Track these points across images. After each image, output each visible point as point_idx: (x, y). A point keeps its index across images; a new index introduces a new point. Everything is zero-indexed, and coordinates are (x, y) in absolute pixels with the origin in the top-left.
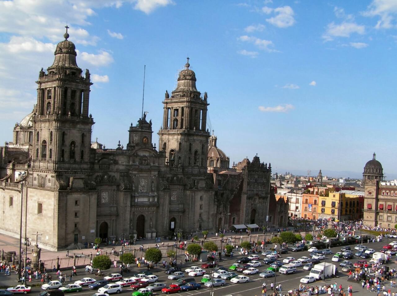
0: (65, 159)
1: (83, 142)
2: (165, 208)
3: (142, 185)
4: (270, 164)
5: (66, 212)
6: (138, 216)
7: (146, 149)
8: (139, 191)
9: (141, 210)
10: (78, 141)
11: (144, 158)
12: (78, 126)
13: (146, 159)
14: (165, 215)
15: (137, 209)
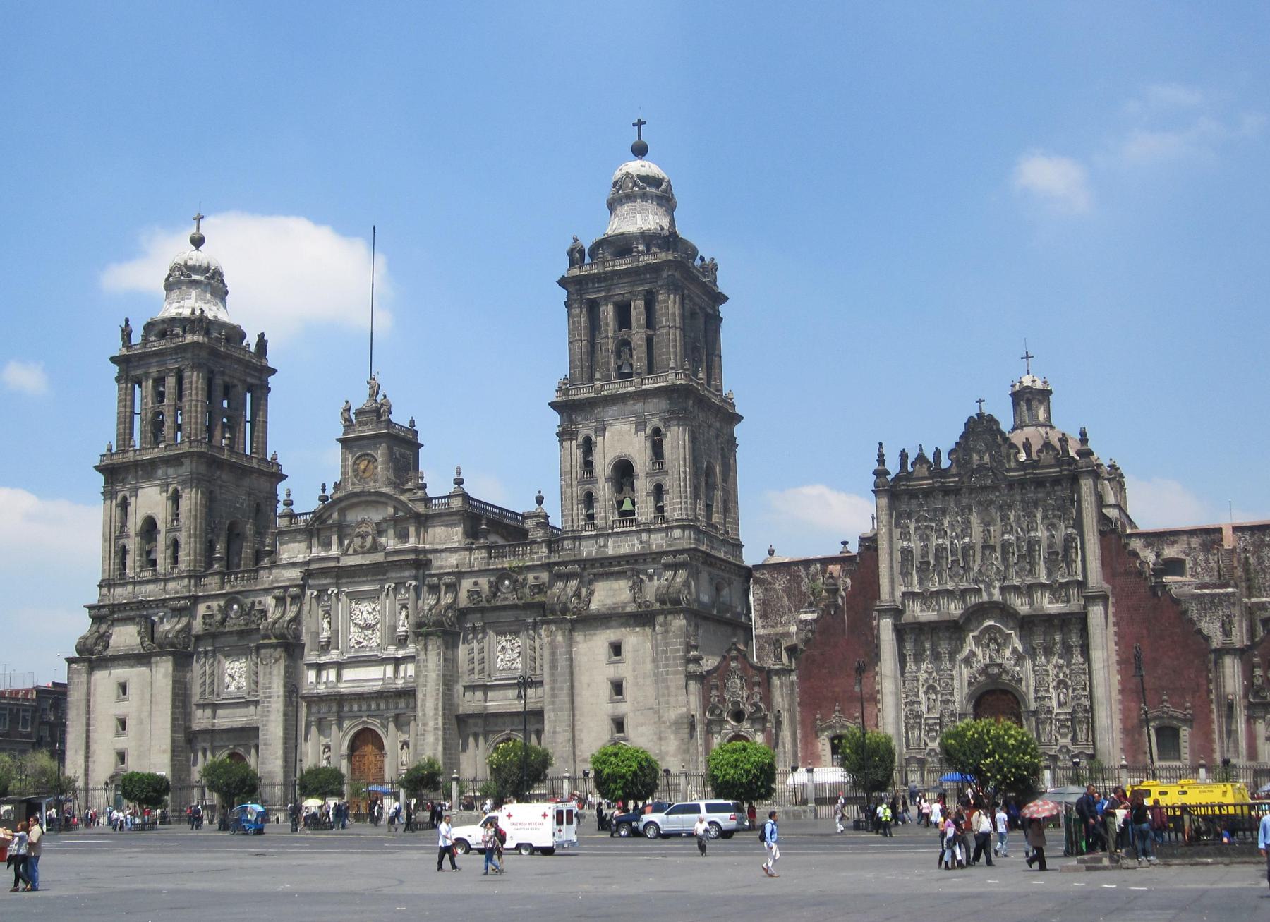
0: (127, 571)
1: (176, 515)
2: (425, 695)
3: (362, 623)
4: (1083, 434)
5: (88, 719)
6: (352, 733)
7: (363, 499)
8: (352, 643)
9: (360, 711)
10: (161, 512)
11: (357, 530)
12: (160, 472)
13: (369, 530)
14: (424, 725)
15: (346, 708)
